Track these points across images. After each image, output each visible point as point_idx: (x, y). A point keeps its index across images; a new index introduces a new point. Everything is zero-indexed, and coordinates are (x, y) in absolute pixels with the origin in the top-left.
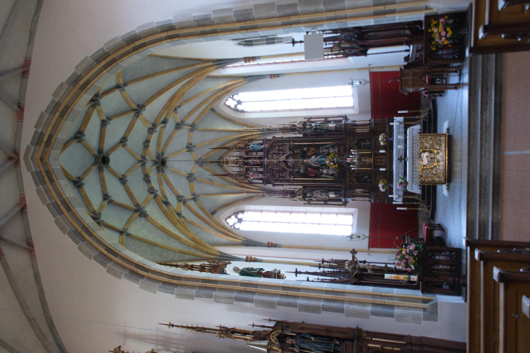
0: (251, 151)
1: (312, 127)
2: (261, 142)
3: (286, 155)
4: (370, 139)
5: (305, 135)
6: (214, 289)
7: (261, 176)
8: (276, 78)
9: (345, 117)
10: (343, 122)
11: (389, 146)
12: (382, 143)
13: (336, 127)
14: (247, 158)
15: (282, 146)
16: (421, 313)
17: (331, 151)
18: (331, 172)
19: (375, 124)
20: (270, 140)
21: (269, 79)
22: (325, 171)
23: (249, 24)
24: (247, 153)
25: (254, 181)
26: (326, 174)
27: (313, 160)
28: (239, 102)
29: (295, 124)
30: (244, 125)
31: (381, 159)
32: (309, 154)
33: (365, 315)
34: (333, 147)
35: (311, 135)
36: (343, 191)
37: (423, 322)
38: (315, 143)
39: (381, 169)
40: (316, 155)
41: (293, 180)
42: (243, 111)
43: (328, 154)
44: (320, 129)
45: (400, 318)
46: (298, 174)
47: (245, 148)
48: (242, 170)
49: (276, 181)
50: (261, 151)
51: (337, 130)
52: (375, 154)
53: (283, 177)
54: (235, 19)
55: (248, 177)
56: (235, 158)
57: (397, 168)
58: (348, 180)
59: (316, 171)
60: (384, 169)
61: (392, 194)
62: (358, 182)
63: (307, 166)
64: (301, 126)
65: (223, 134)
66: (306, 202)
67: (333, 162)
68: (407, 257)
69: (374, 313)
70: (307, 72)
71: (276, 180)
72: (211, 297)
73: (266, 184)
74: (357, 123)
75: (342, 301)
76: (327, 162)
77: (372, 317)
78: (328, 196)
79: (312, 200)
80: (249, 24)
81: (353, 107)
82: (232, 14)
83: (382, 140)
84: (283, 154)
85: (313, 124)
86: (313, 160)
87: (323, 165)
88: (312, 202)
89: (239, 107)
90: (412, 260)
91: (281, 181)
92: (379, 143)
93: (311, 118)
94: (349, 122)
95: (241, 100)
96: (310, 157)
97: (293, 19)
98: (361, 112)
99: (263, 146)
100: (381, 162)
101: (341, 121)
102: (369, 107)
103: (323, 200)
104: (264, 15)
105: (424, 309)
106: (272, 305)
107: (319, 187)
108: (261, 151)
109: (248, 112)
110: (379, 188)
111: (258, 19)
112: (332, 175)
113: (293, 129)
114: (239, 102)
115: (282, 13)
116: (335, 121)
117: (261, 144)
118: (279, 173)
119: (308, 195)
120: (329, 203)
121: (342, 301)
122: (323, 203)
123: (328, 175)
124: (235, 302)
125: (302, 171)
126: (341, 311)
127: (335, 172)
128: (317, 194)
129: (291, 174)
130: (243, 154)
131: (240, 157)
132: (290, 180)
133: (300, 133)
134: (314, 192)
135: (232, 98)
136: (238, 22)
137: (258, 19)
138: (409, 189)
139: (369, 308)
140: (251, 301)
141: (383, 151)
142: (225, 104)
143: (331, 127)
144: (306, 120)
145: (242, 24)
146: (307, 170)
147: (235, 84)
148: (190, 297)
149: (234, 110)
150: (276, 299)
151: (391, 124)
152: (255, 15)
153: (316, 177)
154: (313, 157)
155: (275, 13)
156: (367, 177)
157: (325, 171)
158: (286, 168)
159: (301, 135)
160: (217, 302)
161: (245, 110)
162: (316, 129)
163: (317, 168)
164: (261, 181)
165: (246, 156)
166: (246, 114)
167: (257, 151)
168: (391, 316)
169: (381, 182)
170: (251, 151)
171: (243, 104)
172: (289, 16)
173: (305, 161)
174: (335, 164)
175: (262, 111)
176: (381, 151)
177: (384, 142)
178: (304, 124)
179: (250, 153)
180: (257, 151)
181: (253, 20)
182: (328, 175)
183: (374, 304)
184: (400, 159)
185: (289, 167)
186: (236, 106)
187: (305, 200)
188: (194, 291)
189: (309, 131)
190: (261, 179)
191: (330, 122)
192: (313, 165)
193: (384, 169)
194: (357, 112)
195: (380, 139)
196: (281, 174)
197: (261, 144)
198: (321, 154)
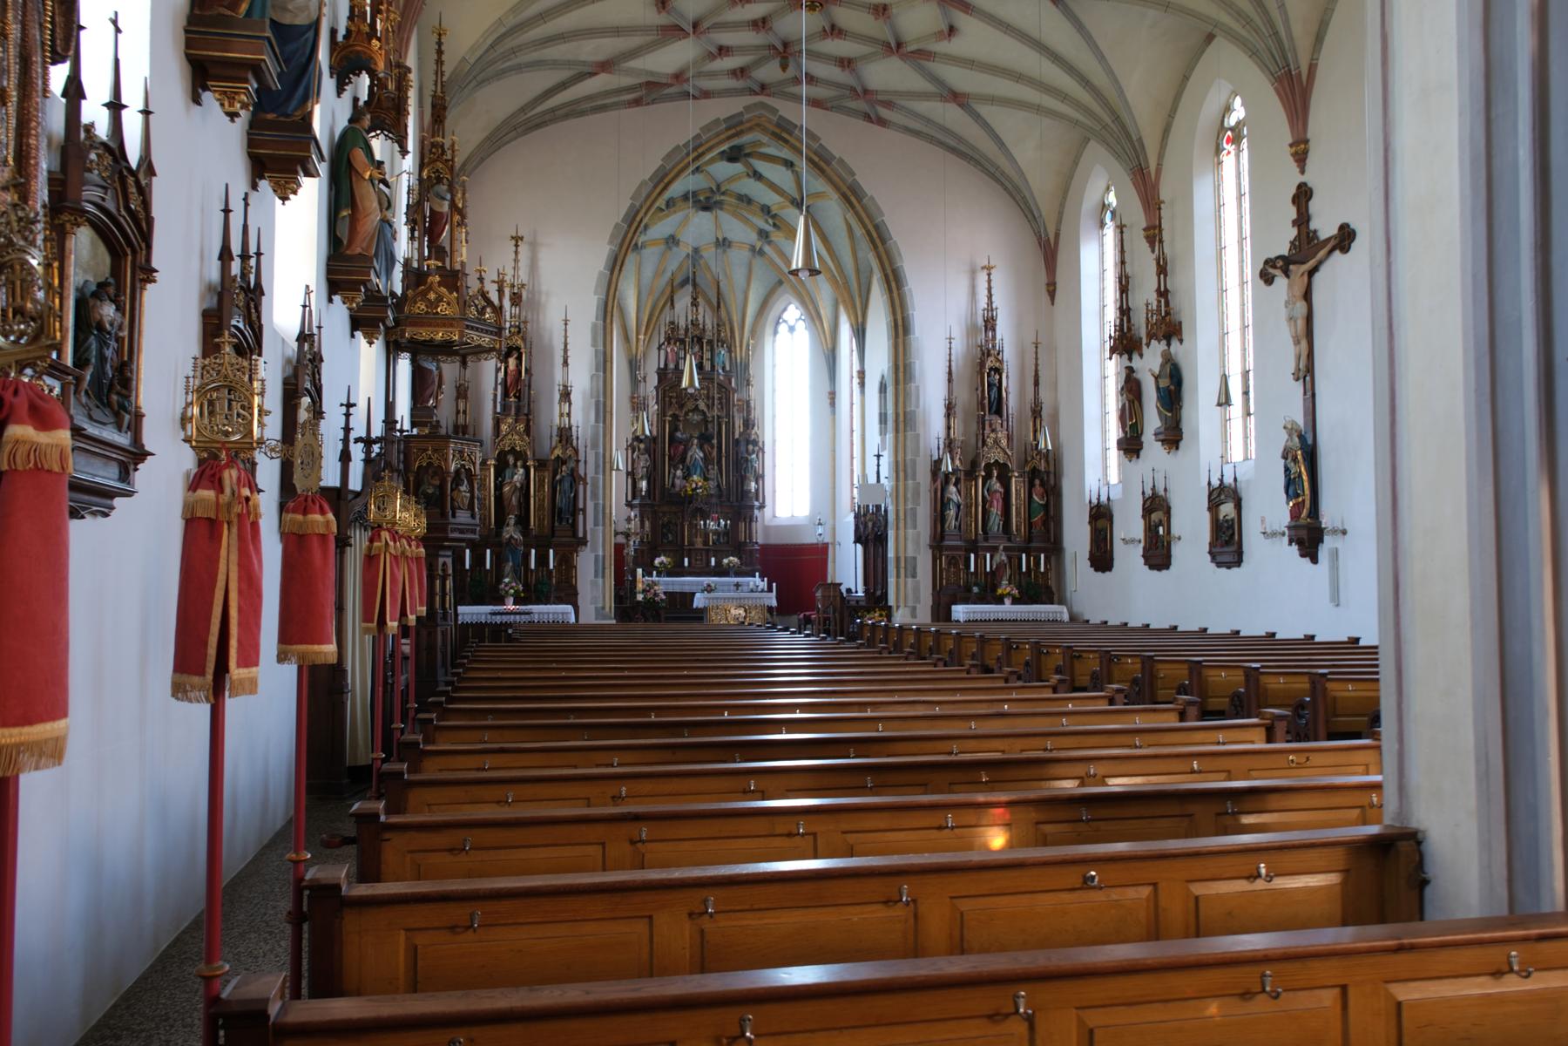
0: (712, 351)
1: (750, 455)
2: (728, 368)
3: (706, 410)
4: (728, 542)
5: (737, 442)
6: (605, 372)
7: (671, 366)
8: (829, 401)
9: (762, 507)
10: (756, 503)
11: (721, 571)
12: (725, 561)
13: (750, 491)
14: (700, 340)
15: (721, 403)
16: (600, 605)
17: (712, 484)
18: (678, 482)
19: (751, 551)
20: (730, 383)
21: (828, 390)
22: (679, 473)
23: (901, 426)
24: (710, 342)
25: (662, 352)
26: (675, 474)
27: (697, 454)
28: (792, 329)
29: (756, 428)
30: (753, 333)
31: (701, 560)
32: (706, 446)
33: (594, 549)
34: (718, 486)
35: (737, 453)
36: (649, 502)
37: (593, 606)
38: (724, 459)
39: (686, 560)
40: (706, 459)
41: (665, 421)
42: (775, 332)
43: (706, 479)
44: (747, 467)
45: (594, 584)
46: (674, 429)
47: (718, 341)
48: (682, 332)
49: (664, 392)
50: (713, 367)
51: (744, 494)
52: (708, 551)
53: (671, 403)
54: (908, 410)
55: (669, 343)
56: (701, 322)
57: (728, 584)
58: (665, 509)
59: (680, 459)
60: (686, 564)
61: (657, 576)
62: (663, 524)
63: (687, 445)
64: (753, 437)
65: (740, 297)
66: (630, 442)
67: (696, 488)
68: (652, 591)
69: (597, 557)
70: (834, 451)
71: (665, 391)
72: (597, 370)
73: (658, 374)
74: (754, 524)
75: (604, 525)
76: (695, 478)
77: (593, 555)
78: (642, 478)
79: (633, 452)
80: (901, 426)
81: (774, 516)
82: (913, 409)
83: (730, 562)
84: (708, 406)
85: (754, 456)
86: (697, 454)
87: (688, 469)
88: (630, 451)
89: (783, 328)
90: (649, 596)
91: (664, 398)
92: (727, 557)
93: (763, 452)
94: (756, 512)
95: (795, 333)
96: (701, 448)
97: (901, 475)
98: (767, 529)
99: (720, 371)
100: (696, 560)
101: (757, 500)
102: (773, 541)
103: (633, 468)
104: (908, 443)
105: (603, 608)
106: (595, 445)
107: (654, 462)
108: (713, 367)
109: (774, 341)
110: (659, 556)
111: (905, 436)
112: (673, 485)
113: (748, 424)
114: (792, 329)
115: (908, 462)
116: (757, 490)
117: (724, 368)
118: (677, 397)
119: (642, 446)
120: (630, 481)
121: (604, 525)
122: (630, 470)
123: (674, 478)
124: (593, 400)
125: (679, 434)
126: (596, 524)
127: (677, 489)
128: (643, 462)
129: (675, 417)
130: (708, 335)
131: (704, 329)
132: (665, 416)
133: (741, 434)
134: (647, 456)
135: (800, 318)
136: (905, 413)
137: (905, 436)
138: (698, 595)
139: (601, 553)
140: (597, 421)
141: (713, 563)
142: (790, 303)
143: (749, 485)
144: (760, 444)
145: (901, 418)
146: (680, 443)
147: (824, 332)
148: (594, 344)
149: (780, 318)
150: (601, 450)
151: (757, 574)
152: (909, 434)
153: (670, 459)
154: (702, 455)
155: (909, 457)
156: (670, 538)
157: (679, 473)
158: (685, 409)
159: (737, 436)
160: (592, 377)
161: (778, 336)
162: (747, 460)
163: (683, 460)
164: (662, 366)
165: (705, 341)
166: (771, 338)
167: (712, 360)
168: (596, 576)
169: (669, 560)
170: (712, 351)
171: (789, 334)
172: (905, 471)
173: (696, 441)
174: (694, 490)
175: (774, 366)
176: (713, 560)
177: (728, 564)
178: (755, 443)
179: (709, 348)
180: (712, 360)
181: (905, 431)
182: (674, 478)
183: (604, 557)
184: (737, 585)
185: (686, 414)
186: (785, 321)
187: (633, 440)
188: (601, 348)
189: (743, 448)
190: (666, 365)
191: (757, 483)
192: (690, 454)
193: (686, 564)
194: (766, 523)
195: (731, 558)
196: (674, 401)
197: (724, 368)
198: (707, 467)
